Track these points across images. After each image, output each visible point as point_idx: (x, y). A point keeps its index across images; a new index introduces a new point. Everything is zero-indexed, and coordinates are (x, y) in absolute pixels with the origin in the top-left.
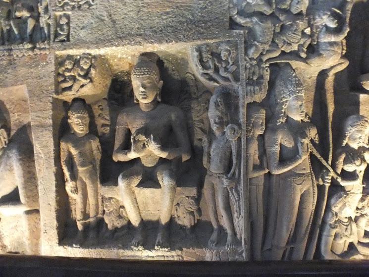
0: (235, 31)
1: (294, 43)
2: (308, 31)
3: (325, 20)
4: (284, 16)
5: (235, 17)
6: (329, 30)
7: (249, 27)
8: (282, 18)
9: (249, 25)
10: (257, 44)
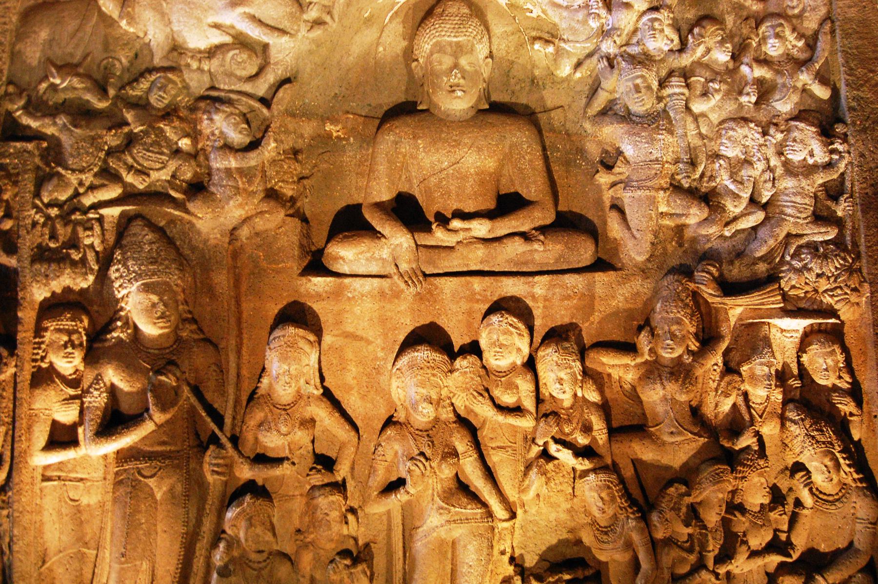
0: (12, 144)
1: (152, 169)
2: (185, 143)
3: (218, 124)
4: (132, 113)
5: (18, 113)
6: (228, 148)
7: (53, 134)
8: (129, 116)
9: (50, 131)
10: (63, 172)
